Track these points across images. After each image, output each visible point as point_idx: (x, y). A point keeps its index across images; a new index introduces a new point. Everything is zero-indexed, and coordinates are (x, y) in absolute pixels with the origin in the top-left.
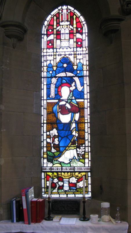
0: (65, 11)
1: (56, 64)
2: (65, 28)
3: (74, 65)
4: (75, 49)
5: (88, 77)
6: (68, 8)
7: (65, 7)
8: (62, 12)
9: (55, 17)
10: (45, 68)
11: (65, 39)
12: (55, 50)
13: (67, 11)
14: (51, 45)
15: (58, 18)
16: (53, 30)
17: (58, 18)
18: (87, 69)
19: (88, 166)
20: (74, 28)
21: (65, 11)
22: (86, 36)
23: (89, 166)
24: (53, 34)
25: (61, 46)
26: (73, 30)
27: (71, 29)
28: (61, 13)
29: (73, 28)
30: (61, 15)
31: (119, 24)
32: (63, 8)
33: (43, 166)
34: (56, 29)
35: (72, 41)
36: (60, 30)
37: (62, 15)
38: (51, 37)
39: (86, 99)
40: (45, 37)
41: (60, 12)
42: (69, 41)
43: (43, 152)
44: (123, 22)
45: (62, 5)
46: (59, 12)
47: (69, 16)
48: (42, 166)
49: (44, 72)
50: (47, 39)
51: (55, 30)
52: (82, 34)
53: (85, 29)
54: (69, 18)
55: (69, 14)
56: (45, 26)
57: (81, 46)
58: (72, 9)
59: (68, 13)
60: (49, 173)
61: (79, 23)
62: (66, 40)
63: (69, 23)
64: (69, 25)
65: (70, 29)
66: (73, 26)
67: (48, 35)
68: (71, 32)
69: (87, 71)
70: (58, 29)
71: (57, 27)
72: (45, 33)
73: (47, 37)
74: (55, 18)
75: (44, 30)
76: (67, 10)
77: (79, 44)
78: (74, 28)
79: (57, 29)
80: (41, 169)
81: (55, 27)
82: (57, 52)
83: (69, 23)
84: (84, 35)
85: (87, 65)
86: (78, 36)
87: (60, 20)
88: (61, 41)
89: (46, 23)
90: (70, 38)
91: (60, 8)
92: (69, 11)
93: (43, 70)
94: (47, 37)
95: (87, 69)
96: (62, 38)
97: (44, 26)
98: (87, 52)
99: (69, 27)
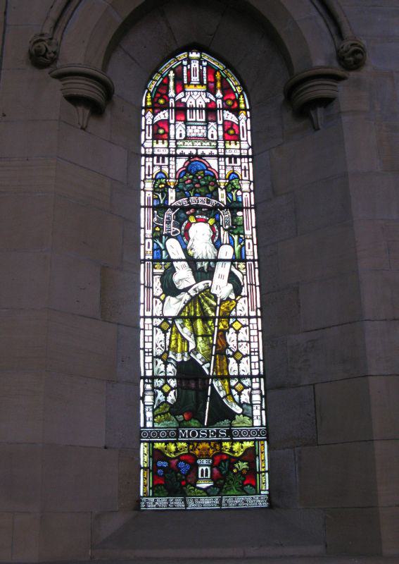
0: (195, 65)
1: (176, 173)
2: (196, 97)
3: (219, 179)
4: (221, 145)
6: (201, 57)
7: (194, 55)
8: (189, 63)
9: (172, 72)
10: (149, 186)
11: (196, 121)
12: (172, 144)
13: (200, 64)
14: (160, 131)
15: (179, 78)
16: (167, 99)
17: (179, 78)
18: (250, 189)
21: (195, 65)
22: (247, 118)
23: (262, 426)
26: (216, 103)
27: (211, 100)
29: (214, 100)
30: (187, 69)
34: (174, 98)
36: (183, 100)
37: (189, 71)
38: (162, 116)
39: (250, 260)
40: (149, 114)
41: (185, 63)
42: (207, 126)
43: (145, 390)
44: (341, 86)
45: (189, 49)
46: (182, 63)
48: (142, 425)
49: (145, 191)
50: (153, 119)
51: (172, 101)
52: (236, 112)
53: (244, 103)
54: (205, 75)
56: (149, 92)
57: (237, 138)
59: (203, 67)
61: (226, 89)
62: (198, 124)
63: (204, 88)
64: (206, 92)
65: (208, 101)
66: (214, 94)
67: (156, 108)
70: (180, 100)
71: (177, 94)
73: (154, 114)
76: (200, 60)
77: (231, 133)
78: (217, 99)
80: (138, 435)
81: (172, 93)
82: (176, 148)
83: (204, 88)
84: (242, 115)
85: (251, 182)
86: (230, 116)
90: (207, 122)
91: (182, 56)
92: (205, 64)
93: (144, 187)
94: (154, 114)
95: (250, 189)
96: (189, 119)
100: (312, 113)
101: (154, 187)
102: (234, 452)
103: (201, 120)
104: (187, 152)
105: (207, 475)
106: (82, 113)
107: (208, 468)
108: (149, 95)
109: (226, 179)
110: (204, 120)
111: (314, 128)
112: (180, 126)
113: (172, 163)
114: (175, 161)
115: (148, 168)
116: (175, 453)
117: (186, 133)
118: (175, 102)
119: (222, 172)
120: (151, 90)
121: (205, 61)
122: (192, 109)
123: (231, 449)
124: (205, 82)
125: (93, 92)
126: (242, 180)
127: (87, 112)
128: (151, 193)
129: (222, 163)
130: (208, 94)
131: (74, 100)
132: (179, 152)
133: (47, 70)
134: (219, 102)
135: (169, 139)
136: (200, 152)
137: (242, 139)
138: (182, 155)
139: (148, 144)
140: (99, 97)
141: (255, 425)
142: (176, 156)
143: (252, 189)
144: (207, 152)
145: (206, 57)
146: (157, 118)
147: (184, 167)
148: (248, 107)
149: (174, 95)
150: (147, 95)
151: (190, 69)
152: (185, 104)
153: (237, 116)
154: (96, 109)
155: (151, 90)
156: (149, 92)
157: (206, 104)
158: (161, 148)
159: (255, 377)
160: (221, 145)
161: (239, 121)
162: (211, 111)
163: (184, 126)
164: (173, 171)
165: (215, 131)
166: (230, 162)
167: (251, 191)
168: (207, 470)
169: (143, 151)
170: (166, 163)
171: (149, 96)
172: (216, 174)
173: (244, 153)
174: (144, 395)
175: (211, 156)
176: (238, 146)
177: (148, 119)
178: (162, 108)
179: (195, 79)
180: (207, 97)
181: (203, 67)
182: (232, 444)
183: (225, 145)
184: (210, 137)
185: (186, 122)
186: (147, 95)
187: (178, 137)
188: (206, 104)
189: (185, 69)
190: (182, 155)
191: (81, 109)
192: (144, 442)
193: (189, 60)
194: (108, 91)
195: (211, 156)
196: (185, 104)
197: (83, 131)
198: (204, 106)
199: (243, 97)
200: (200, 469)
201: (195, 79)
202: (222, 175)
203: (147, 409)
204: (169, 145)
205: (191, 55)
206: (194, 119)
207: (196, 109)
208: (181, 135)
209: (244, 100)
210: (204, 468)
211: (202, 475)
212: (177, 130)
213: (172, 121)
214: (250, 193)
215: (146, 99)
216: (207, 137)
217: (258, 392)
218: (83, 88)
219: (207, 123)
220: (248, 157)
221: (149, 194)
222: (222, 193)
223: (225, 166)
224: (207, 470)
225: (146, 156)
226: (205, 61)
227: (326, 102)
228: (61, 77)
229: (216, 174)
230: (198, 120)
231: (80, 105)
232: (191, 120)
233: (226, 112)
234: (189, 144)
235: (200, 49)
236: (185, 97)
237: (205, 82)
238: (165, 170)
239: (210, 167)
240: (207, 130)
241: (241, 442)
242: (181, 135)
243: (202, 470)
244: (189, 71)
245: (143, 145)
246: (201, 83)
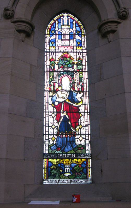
0: (66, 18)
2: (66, 30)
5: (87, 72)
7: (65, 15)
8: (63, 18)
9: (57, 21)
12: (57, 48)
13: (68, 18)
18: (86, 64)
19: (88, 152)
20: (73, 31)
21: (66, 18)
22: (85, 38)
23: (89, 153)
24: (56, 34)
25: (63, 44)
26: (73, 32)
27: (71, 31)
28: (62, 19)
29: (72, 31)
30: (63, 20)
31: (117, 26)
32: (64, 15)
33: (45, 153)
34: (58, 31)
35: (72, 41)
36: (61, 32)
37: (63, 20)
38: (54, 37)
39: (85, 91)
40: (48, 36)
42: (69, 41)
43: (46, 139)
44: (120, 24)
47: (69, 22)
48: (44, 153)
50: (50, 39)
55: (69, 20)
58: (72, 16)
59: (69, 19)
60: (51, 159)
63: (69, 27)
64: (70, 28)
65: (70, 32)
67: (51, 35)
68: (71, 34)
69: (85, 66)
70: (60, 31)
72: (48, 33)
73: (50, 37)
74: (57, 22)
75: (47, 31)
76: (68, 16)
77: (79, 44)
78: (73, 31)
79: (59, 31)
81: (57, 29)
83: (69, 27)
84: (83, 36)
86: (78, 37)
87: (62, 25)
88: (62, 41)
89: (49, 26)
91: (61, 15)
92: (69, 18)
94: (50, 37)
95: (86, 64)
96: (63, 39)
97: (47, 28)
98: (86, 51)
99: (70, 30)
100: (108, 36)
101: (50, 64)
102: (78, 163)
103: (67, 39)
104: (62, 51)
105: (68, 171)
106: (22, 35)
107: (69, 168)
108: (48, 29)
109: (76, 61)
110: (69, 39)
111: (109, 41)
112: (60, 41)
113: (57, 55)
114: (58, 54)
115: (47, 57)
116: (56, 163)
117: (62, 44)
118: (58, 32)
119: (75, 58)
120: (49, 28)
121: (69, 16)
122: (64, 35)
123: (77, 161)
124: (69, 25)
125: (27, 28)
126: (83, 61)
127: (24, 35)
128: (49, 66)
129: (75, 55)
130: (70, 29)
131: (20, 31)
132: (59, 51)
133: (10, 20)
134: (75, 32)
135: (55, 46)
136: (67, 51)
137: (83, 46)
138: (60, 52)
139: (48, 48)
140: (29, 30)
141: (87, 152)
142: (58, 52)
143: (87, 64)
144: (70, 50)
145: (70, 15)
146: (51, 38)
147: (61, 56)
148: (85, 34)
149: (58, 30)
150: (47, 30)
151: (64, 20)
152: (62, 33)
153: (81, 37)
154: (28, 35)
155: (49, 28)
156: (48, 28)
157: (70, 33)
158: (52, 49)
159: (87, 135)
160: (75, 48)
161: (82, 39)
162: (71, 36)
163: (61, 41)
164: (57, 58)
165: (73, 43)
166: (79, 54)
167: (86, 65)
168: (68, 169)
169: (46, 50)
170: (55, 55)
171: (48, 30)
172: (73, 58)
173: (84, 51)
174: (45, 141)
175: (71, 52)
176: (81, 48)
177: (48, 38)
178: (53, 34)
179: (66, 24)
180: (70, 30)
181: (69, 19)
182: (78, 160)
183: (76, 48)
184: (71, 45)
185: (62, 40)
186: (47, 30)
187: (59, 45)
188: (70, 33)
189: (62, 20)
190: (60, 52)
191: (22, 34)
192: (45, 158)
193: (63, 16)
194: (33, 28)
195: (71, 52)
196: (62, 33)
197: (22, 42)
198: (69, 34)
199: (84, 30)
200: (66, 168)
201: (66, 24)
202: (75, 60)
203: (46, 146)
204: (55, 48)
205: (64, 15)
206: (65, 39)
207: (66, 35)
208: (60, 45)
209: (84, 31)
210: (67, 168)
211: (67, 171)
212: (59, 43)
213: (57, 40)
214: (85, 66)
215: (47, 31)
216: (70, 45)
217: (88, 140)
218: (23, 26)
219: (69, 40)
220: (85, 52)
221: (48, 67)
222: (75, 66)
223: (77, 56)
224: (68, 169)
225: (47, 52)
226: (69, 16)
227: (114, 32)
228: (14, 22)
229: (73, 58)
230: (66, 39)
231: (22, 33)
232: (64, 39)
233: (77, 36)
234: (63, 48)
235: (68, 12)
236: (62, 30)
237: (69, 25)
238: (54, 57)
239: (71, 56)
240: (70, 42)
241: (81, 159)
242: (60, 45)
243: (67, 169)
244: (63, 20)
245: (46, 48)
246: (68, 25)
